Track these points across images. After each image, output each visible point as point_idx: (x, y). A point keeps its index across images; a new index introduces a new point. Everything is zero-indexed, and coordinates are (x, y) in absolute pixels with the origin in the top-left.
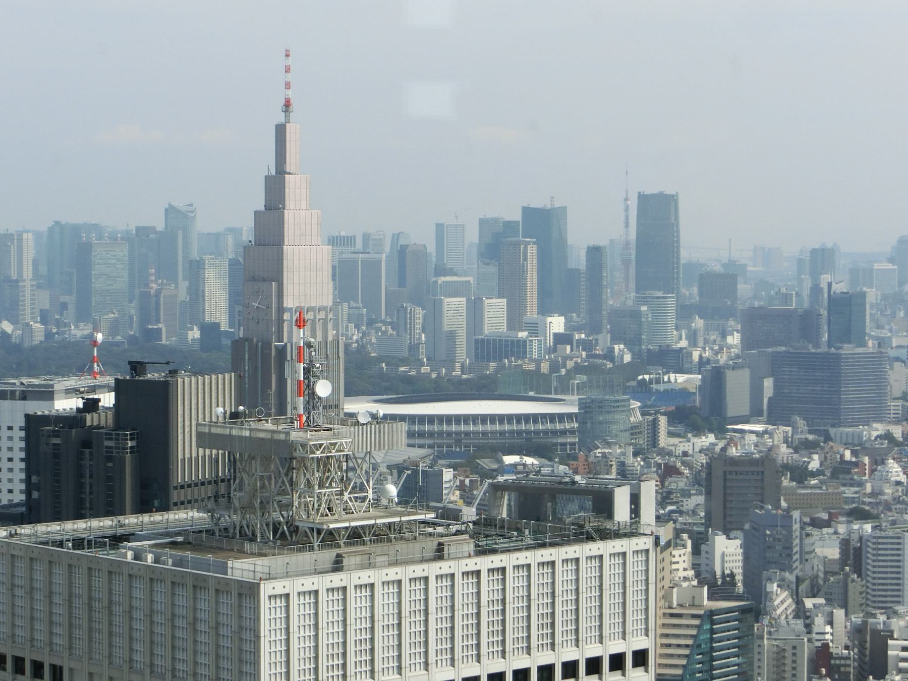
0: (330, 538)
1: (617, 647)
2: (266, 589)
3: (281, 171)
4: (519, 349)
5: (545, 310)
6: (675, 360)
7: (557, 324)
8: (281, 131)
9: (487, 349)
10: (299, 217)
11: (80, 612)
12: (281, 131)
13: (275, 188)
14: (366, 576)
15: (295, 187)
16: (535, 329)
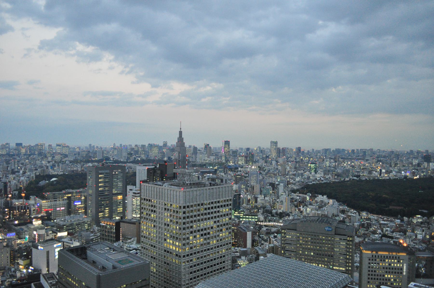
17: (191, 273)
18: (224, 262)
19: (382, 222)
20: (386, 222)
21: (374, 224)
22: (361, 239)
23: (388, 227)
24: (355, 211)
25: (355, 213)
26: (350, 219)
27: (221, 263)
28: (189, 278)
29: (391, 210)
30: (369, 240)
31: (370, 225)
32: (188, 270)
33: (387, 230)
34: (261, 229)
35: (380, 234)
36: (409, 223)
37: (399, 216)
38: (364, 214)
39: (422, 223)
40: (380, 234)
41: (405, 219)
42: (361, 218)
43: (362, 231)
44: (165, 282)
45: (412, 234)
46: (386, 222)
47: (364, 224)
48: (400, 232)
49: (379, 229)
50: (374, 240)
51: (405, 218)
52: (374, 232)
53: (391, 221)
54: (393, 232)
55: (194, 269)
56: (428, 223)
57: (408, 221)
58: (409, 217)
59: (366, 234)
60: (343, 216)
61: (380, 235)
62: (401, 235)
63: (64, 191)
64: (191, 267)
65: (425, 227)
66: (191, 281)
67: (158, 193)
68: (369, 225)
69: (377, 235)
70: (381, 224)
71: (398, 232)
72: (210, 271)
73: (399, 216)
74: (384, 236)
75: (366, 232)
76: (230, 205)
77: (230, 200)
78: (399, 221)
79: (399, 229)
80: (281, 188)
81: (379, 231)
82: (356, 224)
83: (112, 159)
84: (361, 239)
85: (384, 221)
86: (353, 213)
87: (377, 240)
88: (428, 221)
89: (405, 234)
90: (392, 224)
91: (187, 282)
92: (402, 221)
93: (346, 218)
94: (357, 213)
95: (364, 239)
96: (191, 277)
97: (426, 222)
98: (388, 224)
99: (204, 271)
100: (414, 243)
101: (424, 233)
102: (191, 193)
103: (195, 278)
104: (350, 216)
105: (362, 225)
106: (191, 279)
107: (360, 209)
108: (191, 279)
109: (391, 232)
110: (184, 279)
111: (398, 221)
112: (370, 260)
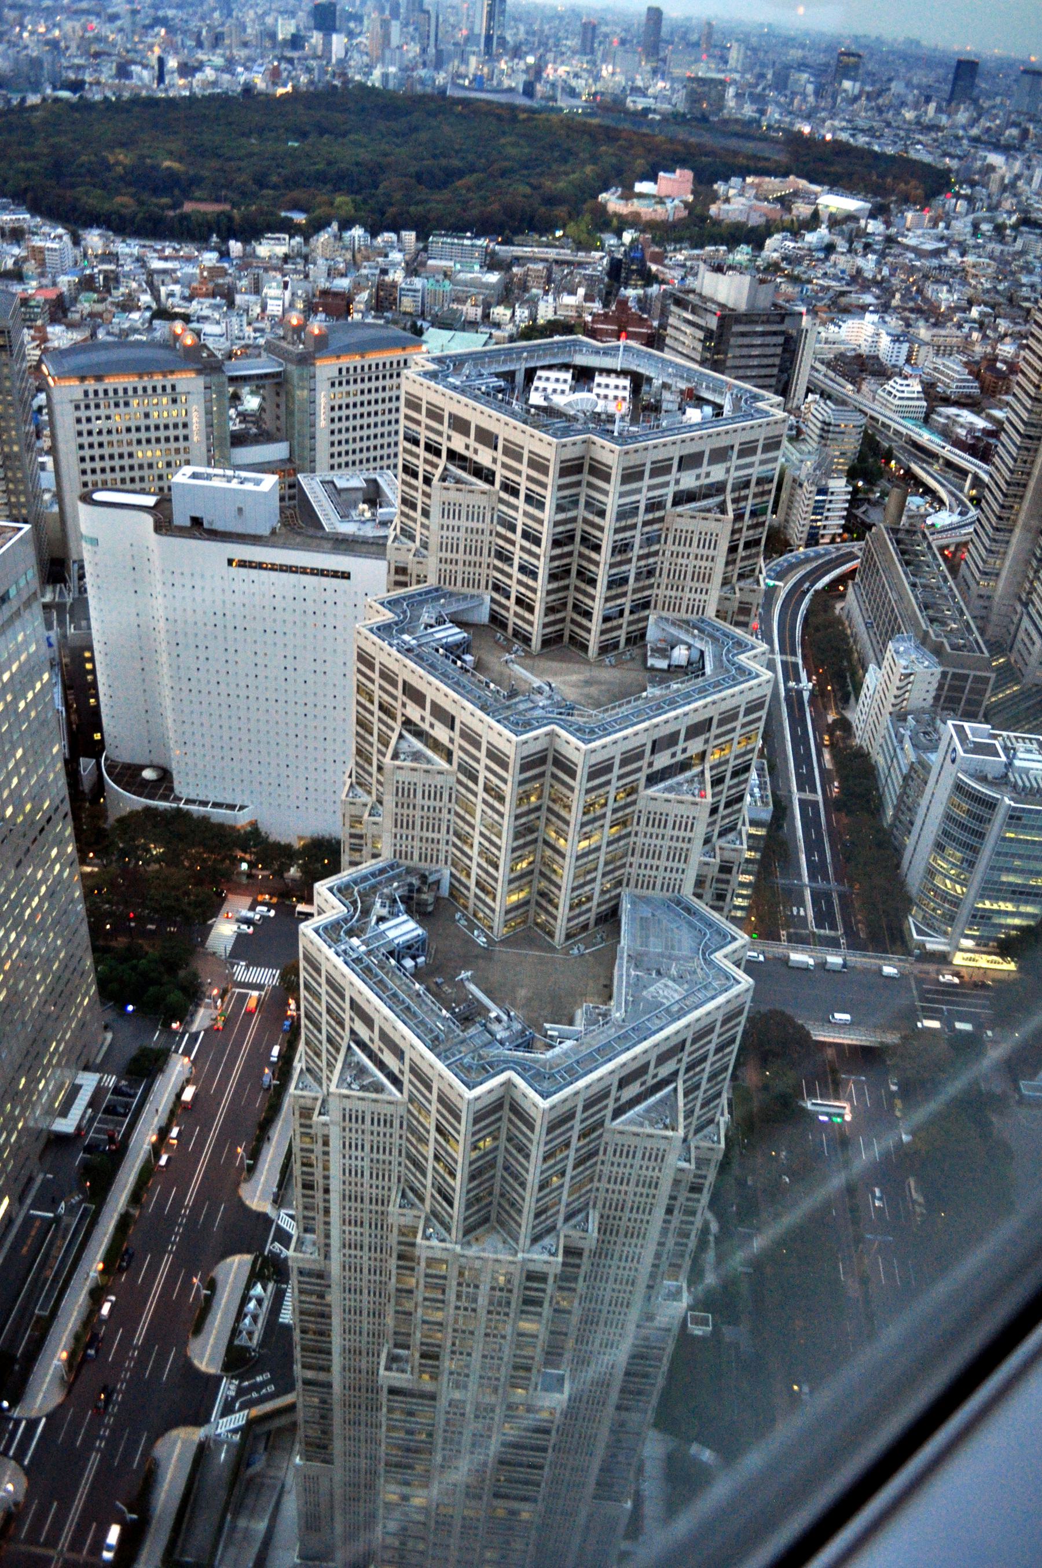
19: (157, 264)
20: (169, 265)
21: (127, 275)
22: (77, 336)
23: (176, 282)
24: (60, 231)
25: (60, 237)
26: (42, 263)
29: (184, 217)
30: (108, 333)
31: (117, 280)
33: (172, 293)
35: (148, 308)
36: (247, 261)
37: (215, 238)
38: (94, 239)
39: (286, 258)
40: (148, 308)
41: (235, 247)
42: (85, 255)
43: (86, 304)
45: (252, 298)
46: (169, 265)
47: (92, 277)
48: (214, 296)
49: (144, 291)
50: (125, 333)
51: (232, 243)
52: (128, 305)
53: (189, 259)
54: (189, 299)
56: (306, 259)
57: (244, 256)
58: (246, 241)
59: (100, 315)
60: (16, 251)
61: (148, 314)
62: (217, 307)
65: (296, 271)
68: (112, 280)
69: (135, 316)
70: (151, 273)
71: (206, 295)
73: (215, 238)
74: (163, 314)
75: (99, 307)
78: (214, 255)
79: (211, 286)
81: (146, 299)
82: (65, 282)
84: (77, 336)
85: (166, 259)
86: (52, 238)
87: (136, 331)
88: (305, 250)
89: (231, 304)
90: (190, 269)
92: (224, 255)
93: (25, 259)
94: (66, 238)
95: (94, 335)
97: (299, 255)
98: (174, 271)
100: (256, 330)
101: (288, 294)
104: (41, 250)
105: (87, 284)
107: (75, 219)
109: (184, 298)
111: (210, 258)
112: (77, 408)
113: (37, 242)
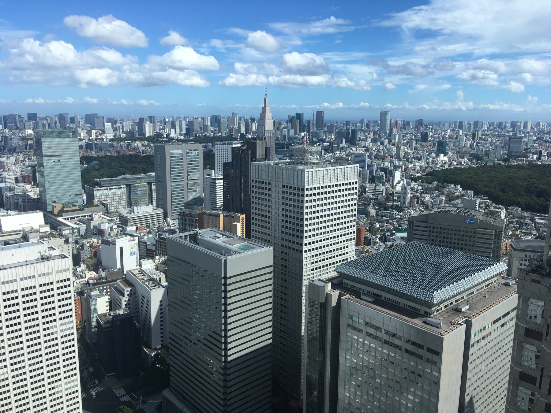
0: (310, 164)
1: (353, 181)
2: (306, 170)
3: (265, 106)
4: (296, 138)
5: (300, 132)
6: (324, 141)
7: (303, 134)
8: (265, 99)
9: (291, 138)
10: (268, 115)
11: (274, 174)
12: (265, 99)
13: (264, 109)
14: (315, 169)
15: (268, 109)
16: (299, 135)
17: (313, 263)
18: (347, 253)
24: (501, 206)
27: (344, 254)
28: (311, 269)
32: (309, 259)
34: (372, 226)
44: (282, 273)
55: (316, 259)
63: (120, 177)
64: (313, 256)
66: (313, 272)
67: (274, 174)
72: (332, 262)
76: (356, 188)
77: (356, 183)
80: (398, 175)
83: (165, 136)
91: (309, 273)
96: (312, 268)
99: (326, 262)
102: (332, 171)
103: (316, 269)
106: (313, 270)
108: (313, 270)
110: (305, 270)
113: (492, 209)
